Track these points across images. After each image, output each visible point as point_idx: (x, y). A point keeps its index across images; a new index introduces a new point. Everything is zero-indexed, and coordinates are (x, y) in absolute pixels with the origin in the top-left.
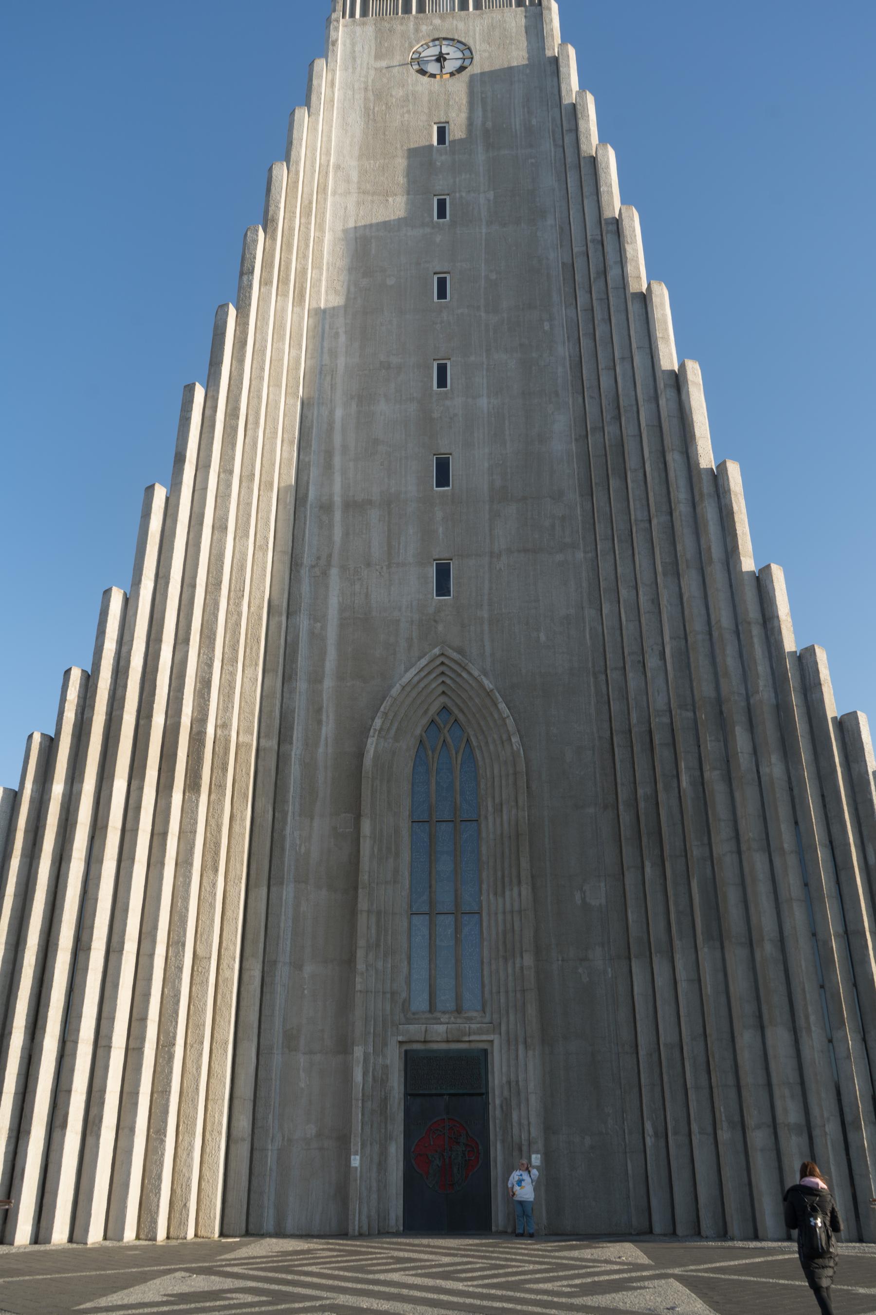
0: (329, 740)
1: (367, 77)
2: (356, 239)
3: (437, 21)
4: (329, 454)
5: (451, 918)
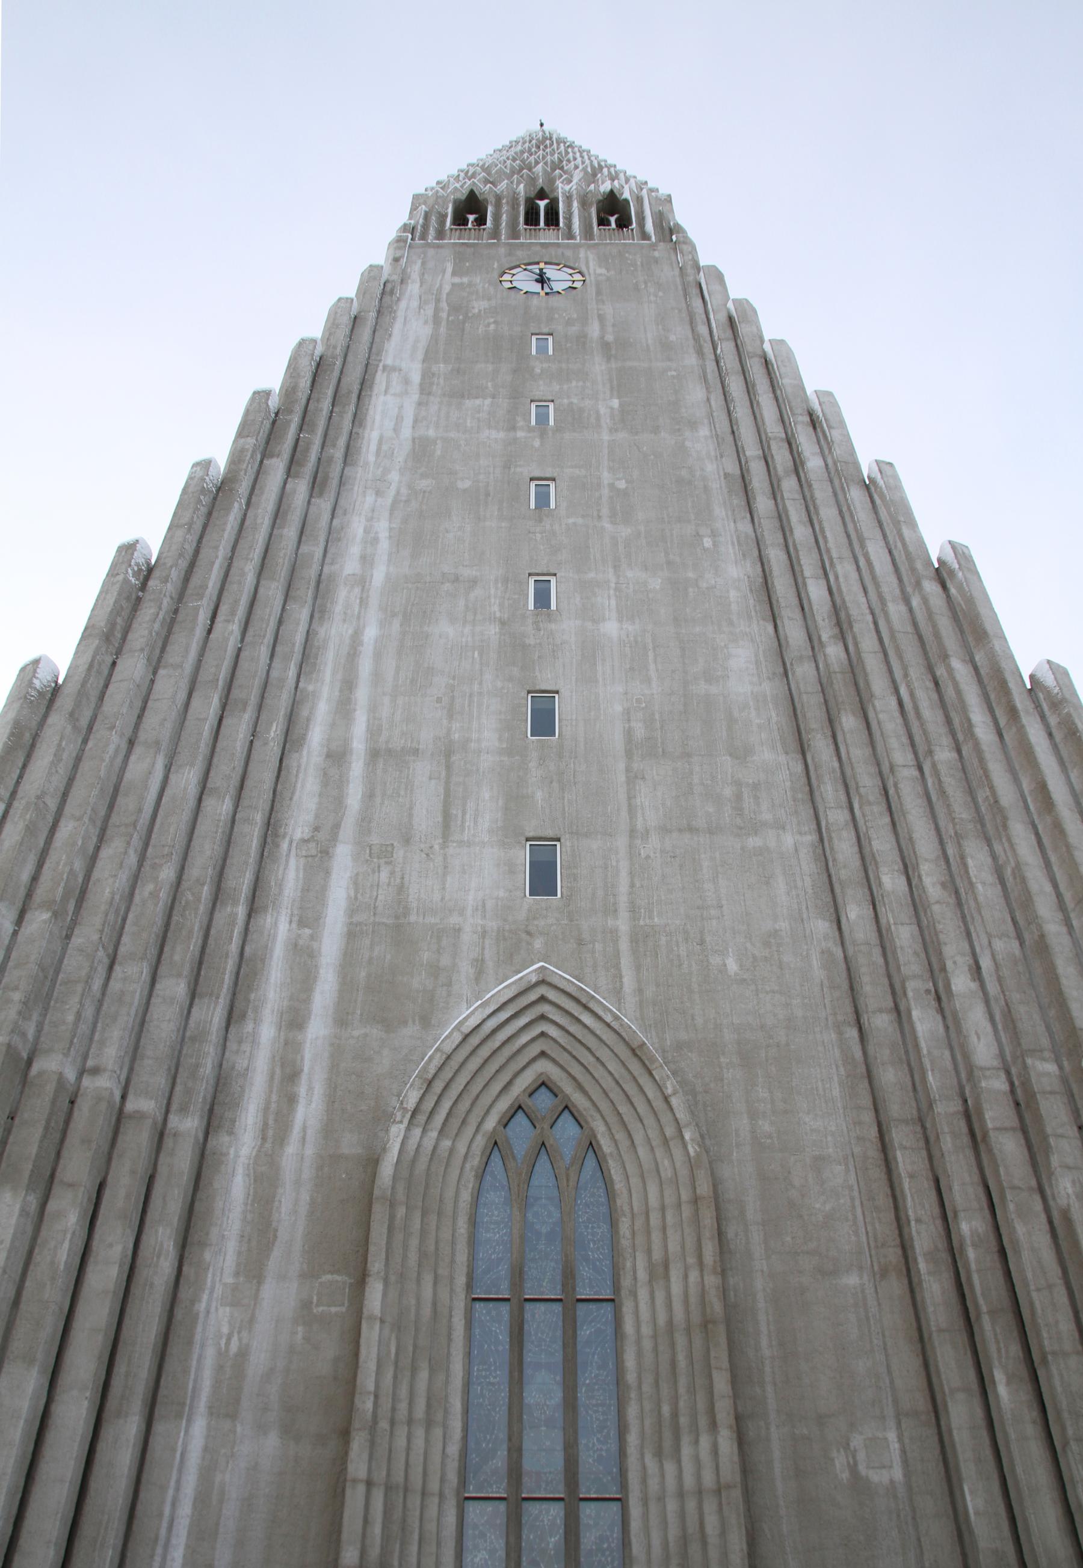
0: (309, 1132)
2: (414, 439)
4: (349, 685)
5: (556, 1512)
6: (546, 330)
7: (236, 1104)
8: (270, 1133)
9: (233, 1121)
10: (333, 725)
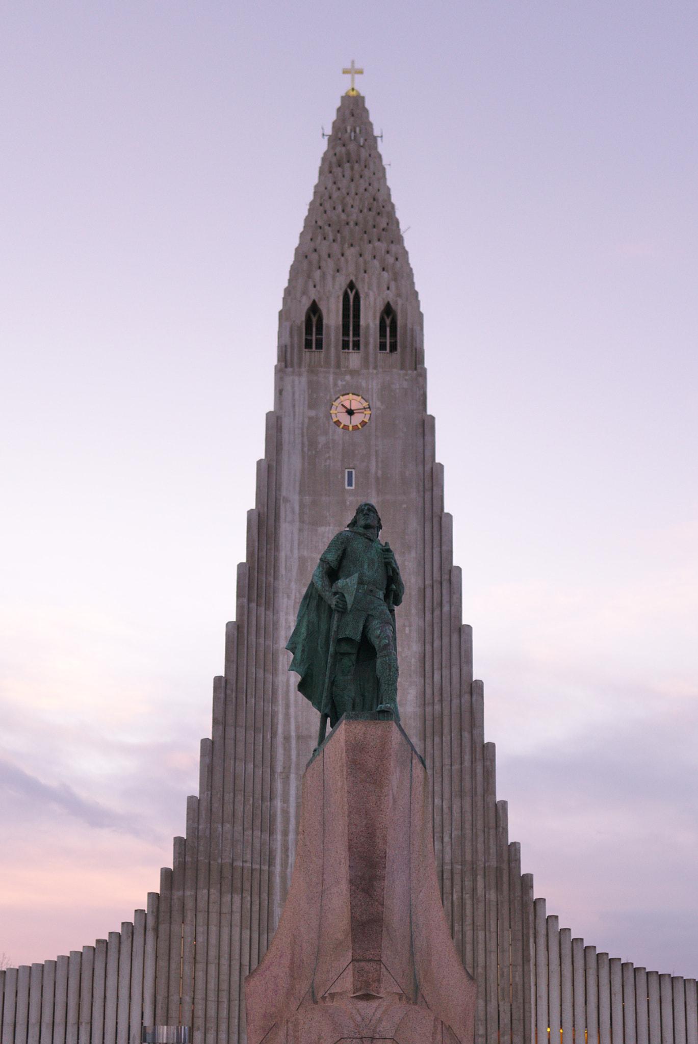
1: (303, 424)
3: (348, 378)
4: (287, 706)
6: (351, 466)
7: (274, 859)
8: (283, 866)
9: (275, 863)
10: (284, 726)
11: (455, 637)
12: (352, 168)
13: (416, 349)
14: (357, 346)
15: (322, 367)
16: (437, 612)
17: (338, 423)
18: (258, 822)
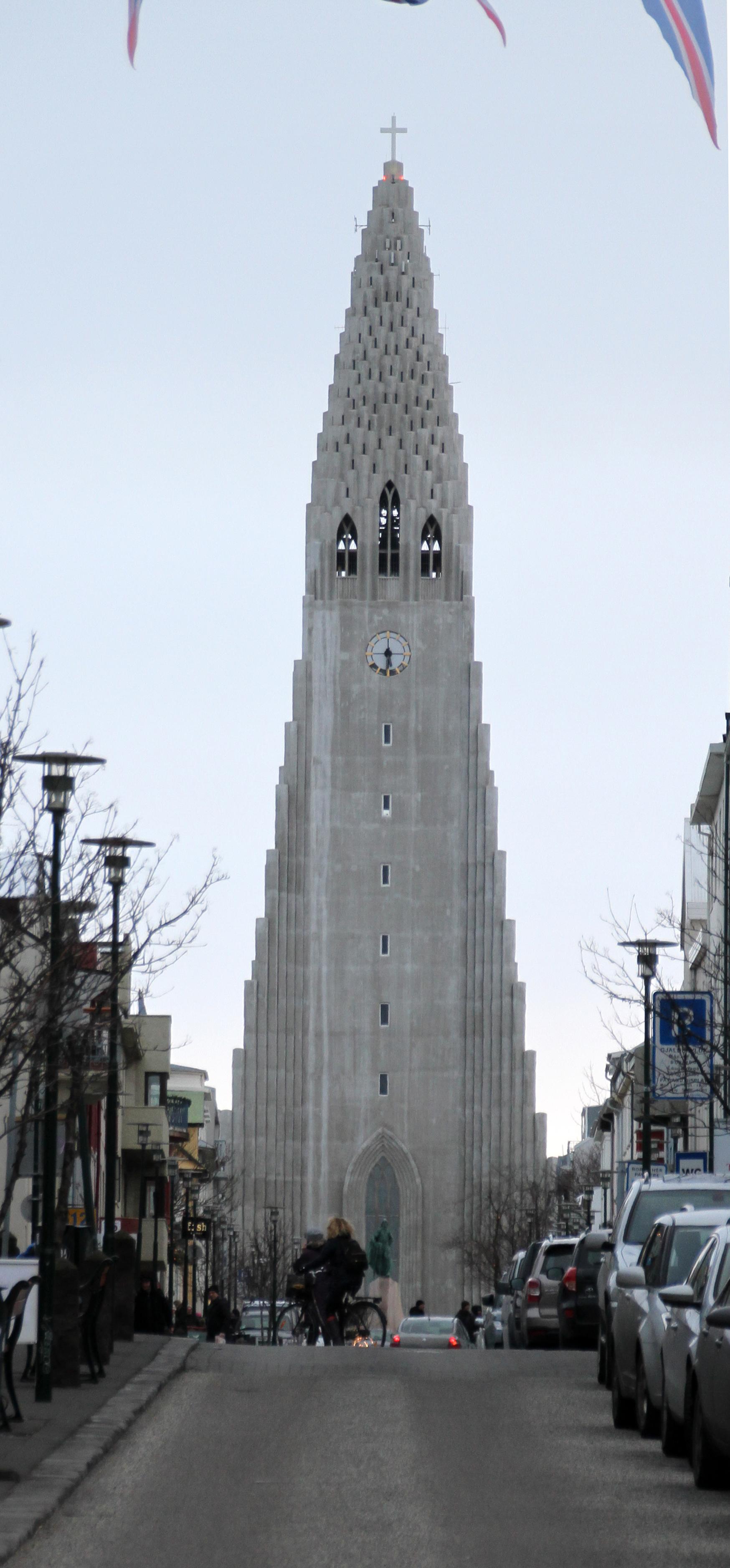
3: (385, 612)
4: (319, 999)
11: (497, 933)
12: (391, 308)
13: (463, 572)
14: (395, 569)
15: (356, 598)
16: (479, 898)
17: (374, 666)
18: (290, 1131)
